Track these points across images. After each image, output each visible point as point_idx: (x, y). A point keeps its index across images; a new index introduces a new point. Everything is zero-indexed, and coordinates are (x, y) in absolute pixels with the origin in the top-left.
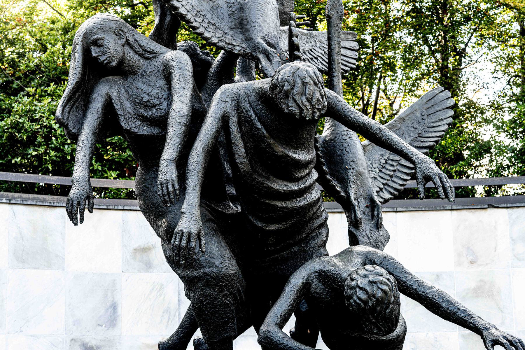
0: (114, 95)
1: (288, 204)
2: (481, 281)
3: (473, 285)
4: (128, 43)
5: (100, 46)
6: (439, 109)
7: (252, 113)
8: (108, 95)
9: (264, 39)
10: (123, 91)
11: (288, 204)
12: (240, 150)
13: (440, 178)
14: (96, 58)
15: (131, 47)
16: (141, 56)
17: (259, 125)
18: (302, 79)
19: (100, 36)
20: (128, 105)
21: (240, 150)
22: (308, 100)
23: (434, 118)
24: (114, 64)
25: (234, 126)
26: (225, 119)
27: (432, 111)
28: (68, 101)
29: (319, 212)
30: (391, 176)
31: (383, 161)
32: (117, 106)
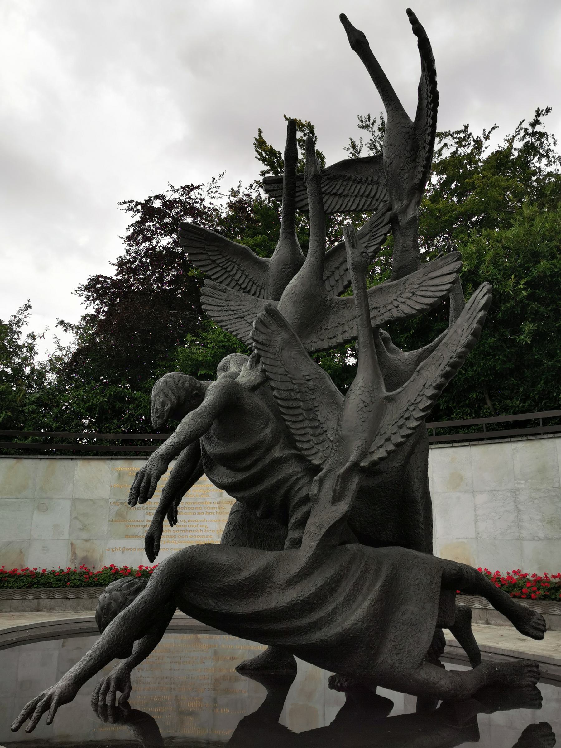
29: (293, 492)
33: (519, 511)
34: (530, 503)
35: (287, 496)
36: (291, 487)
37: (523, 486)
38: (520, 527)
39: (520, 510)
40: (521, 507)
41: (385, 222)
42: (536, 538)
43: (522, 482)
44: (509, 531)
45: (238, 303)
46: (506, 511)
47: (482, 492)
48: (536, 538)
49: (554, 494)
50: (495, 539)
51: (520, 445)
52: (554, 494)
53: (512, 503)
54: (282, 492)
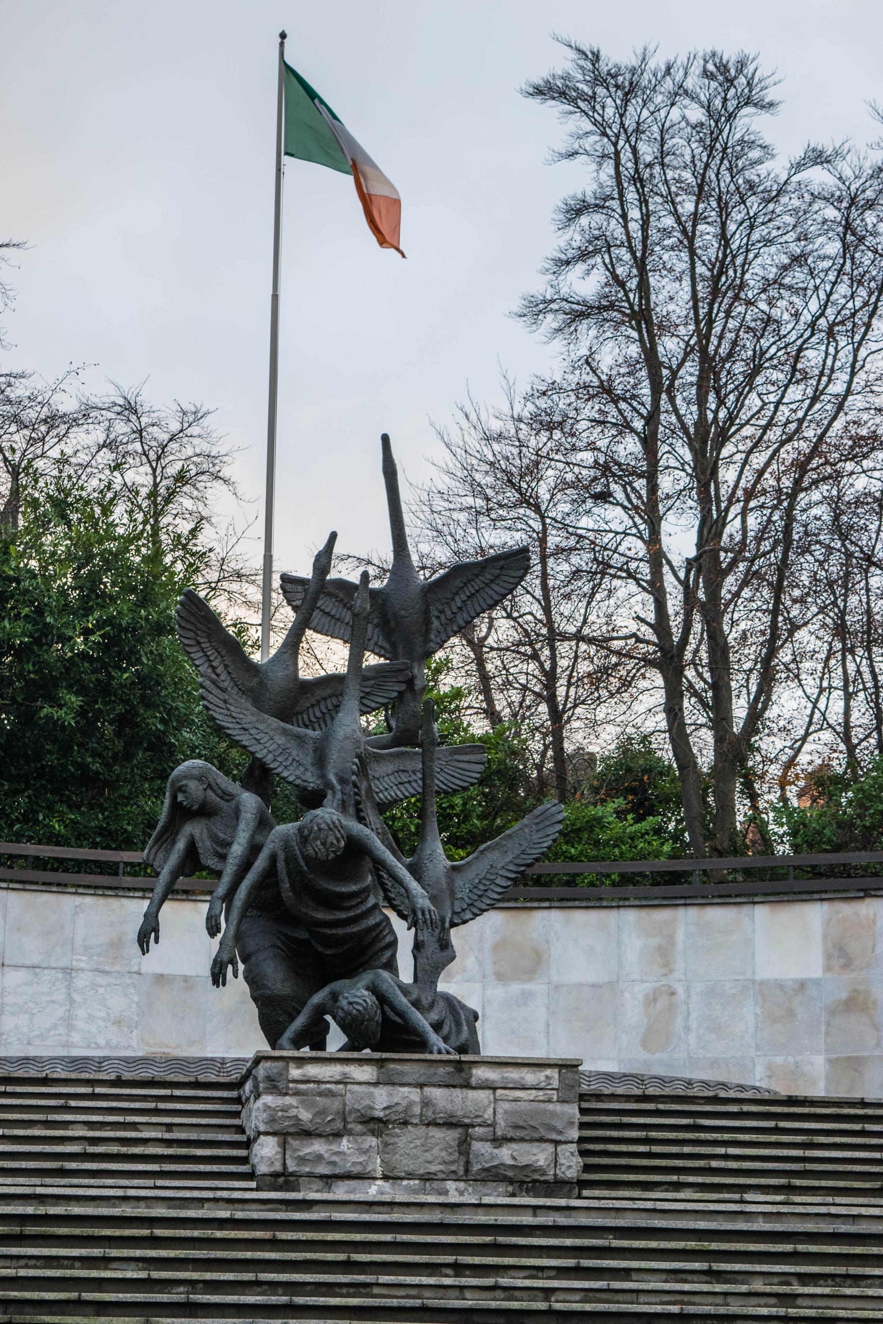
0: (197, 836)
1: (340, 931)
2: (855, 990)
3: (844, 995)
4: (210, 786)
5: (184, 792)
6: (548, 823)
7: (298, 853)
8: (192, 836)
9: (336, 775)
10: (205, 831)
11: (340, 931)
12: (286, 885)
13: (430, 911)
14: (181, 803)
15: (214, 791)
16: (221, 798)
17: (303, 864)
18: (318, 825)
19: (184, 782)
20: (208, 843)
21: (286, 885)
22: (322, 844)
23: (541, 834)
24: (195, 808)
25: (281, 865)
26: (273, 858)
27: (541, 826)
28: (154, 844)
30: (480, 896)
31: (476, 881)
32: (199, 845)
33: (72, 1002)
34: (92, 992)
35: (377, 939)
36: (381, 932)
37: (83, 965)
38: (70, 1027)
39: (75, 1001)
40: (77, 997)
41: (401, 678)
42: (93, 1045)
43: (84, 958)
44: (52, 1033)
45: (238, 710)
46: (52, 1002)
47: (17, 967)
48: (93, 1045)
49: (129, 981)
50: (29, 1044)
51: (89, 900)
52: (129, 981)
53: (64, 990)
54: (374, 934)
